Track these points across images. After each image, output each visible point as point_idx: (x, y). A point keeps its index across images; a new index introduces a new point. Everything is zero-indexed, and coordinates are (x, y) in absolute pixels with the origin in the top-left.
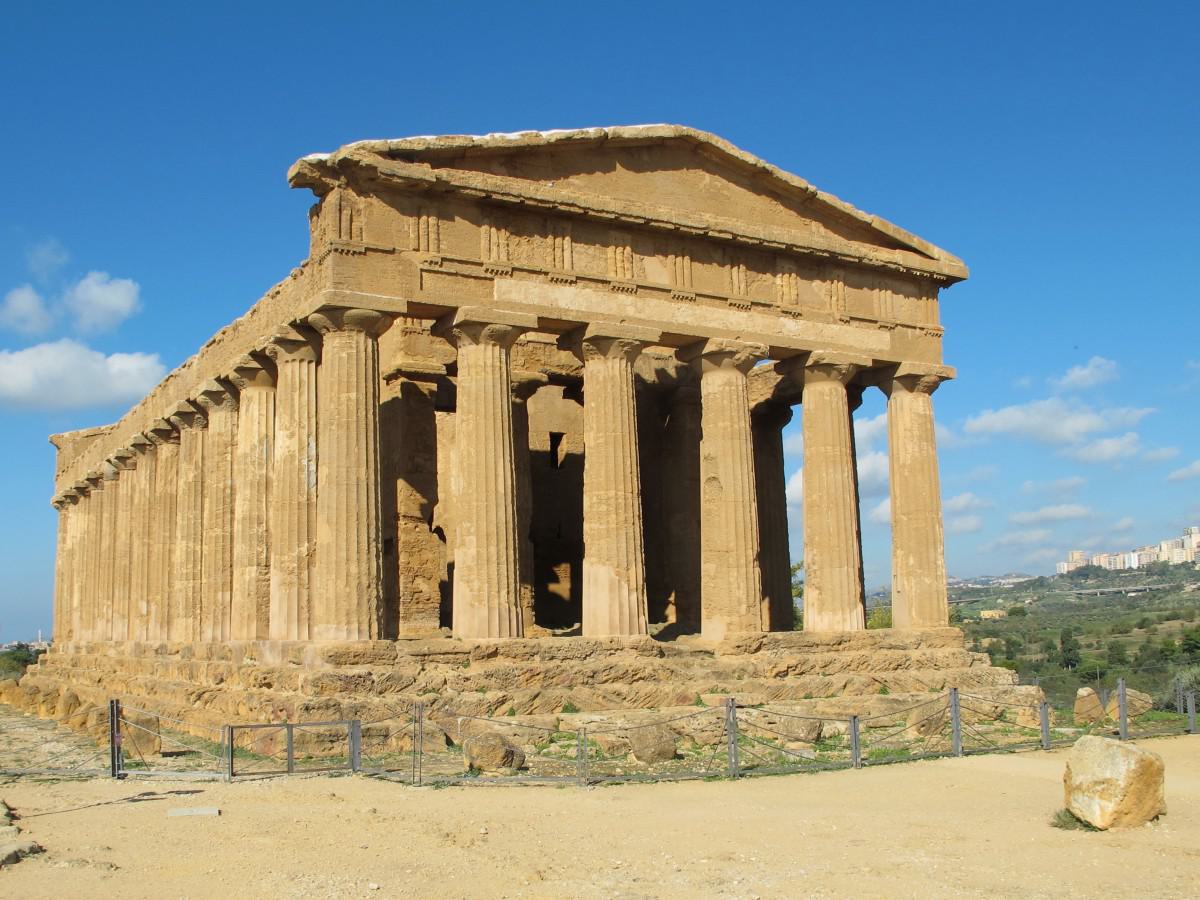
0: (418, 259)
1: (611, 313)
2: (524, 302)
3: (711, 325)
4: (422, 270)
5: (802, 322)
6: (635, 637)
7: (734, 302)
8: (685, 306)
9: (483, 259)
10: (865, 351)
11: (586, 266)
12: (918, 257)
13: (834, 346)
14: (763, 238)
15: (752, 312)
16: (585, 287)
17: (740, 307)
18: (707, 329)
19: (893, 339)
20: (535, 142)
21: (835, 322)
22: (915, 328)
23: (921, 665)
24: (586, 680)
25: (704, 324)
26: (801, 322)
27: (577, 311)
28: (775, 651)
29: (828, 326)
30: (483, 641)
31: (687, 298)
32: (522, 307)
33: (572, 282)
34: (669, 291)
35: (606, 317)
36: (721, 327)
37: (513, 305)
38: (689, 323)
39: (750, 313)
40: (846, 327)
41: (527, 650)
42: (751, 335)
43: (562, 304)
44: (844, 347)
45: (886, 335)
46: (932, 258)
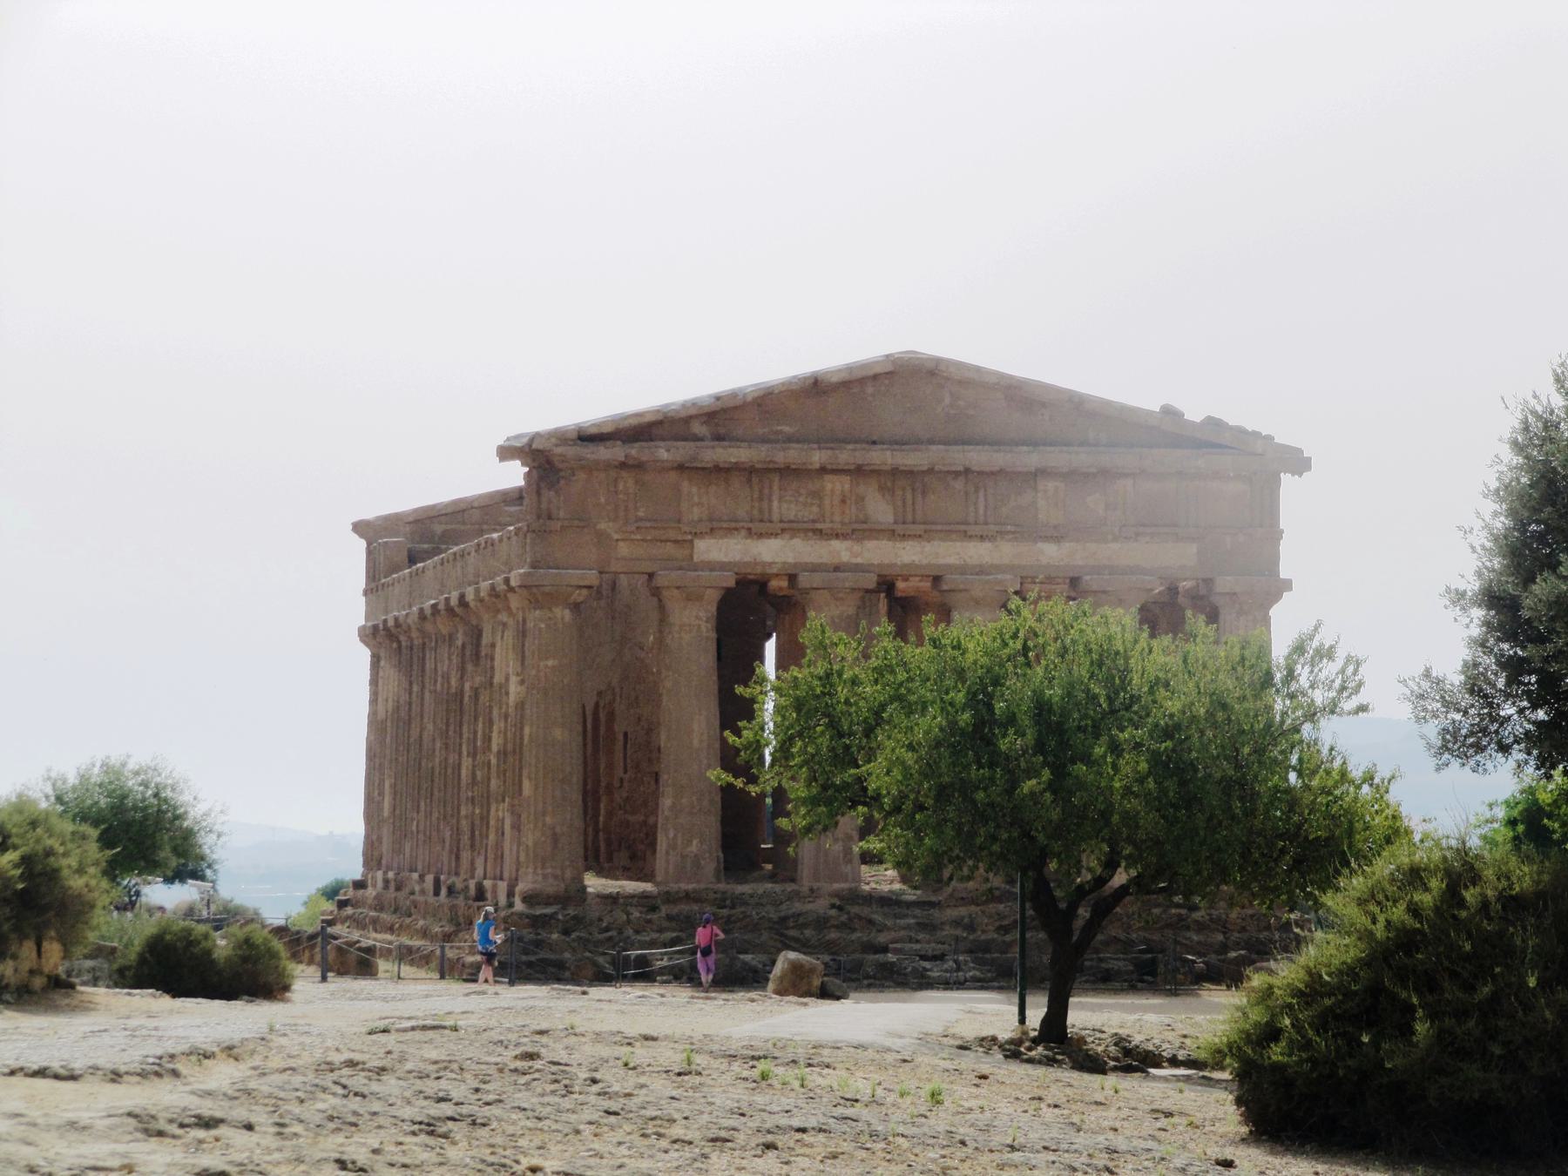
1: (820, 561)
2: (724, 560)
4: (617, 540)
5: (1067, 545)
6: (836, 886)
7: (974, 534)
11: (796, 516)
16: (792, 538)
17: (982, 538)
21: (1115, 539)
23: (1201, 927)
24: (771, 925)
26: (1067, 546)
27: (785, 563)
32: (723, 566)
33: (777, 535)
36: (958, 562)
38: (917, 562)
41: (715, 896)
43: (767, 558)
45: (1194, 548)
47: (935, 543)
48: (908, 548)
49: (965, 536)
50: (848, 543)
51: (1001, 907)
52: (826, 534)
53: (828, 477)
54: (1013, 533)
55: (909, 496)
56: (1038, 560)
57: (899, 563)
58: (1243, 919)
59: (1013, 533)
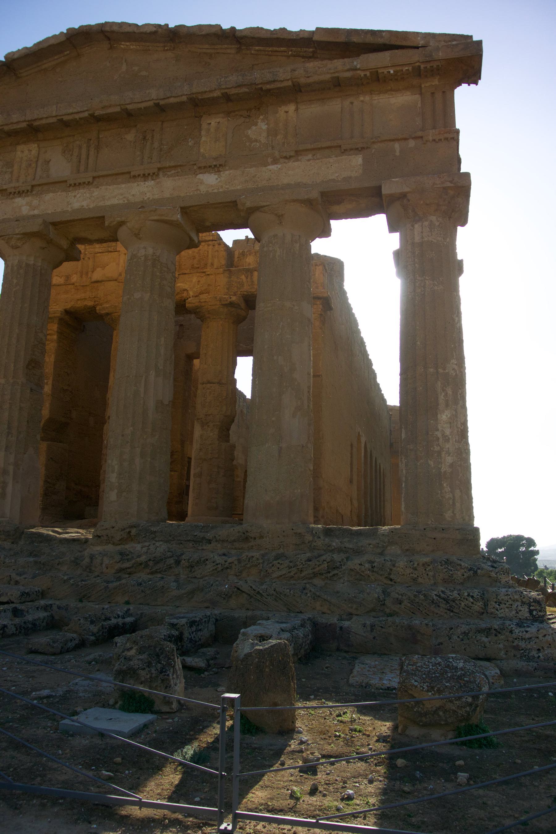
1: (5, 217)
3: (108, 203)
5: (227, 172)
7: (137, 173)
12: (387, 55)
14: (155, 98)
17: (145, 177)
22: (406, 139)
25: (101, 204)
26: (226, 174)
28: (147, 544)
29: (264, 169)
31: (84, 183)
34: (66, 181)
36: (121, 202)
39: (158, 180)
45: (358, 160)
46: (417, 48)
47: (103, 187)
48: (78, 196)
49: (130, 178)
50: (28, 199)
51: (138, 547)
52: (10, 193)
53: (20, 148)
54: (175, 167)
55: (84, 151)
56: (197, 190)
57: (70, 210)
58: (415, 569)
59: (175, 167)
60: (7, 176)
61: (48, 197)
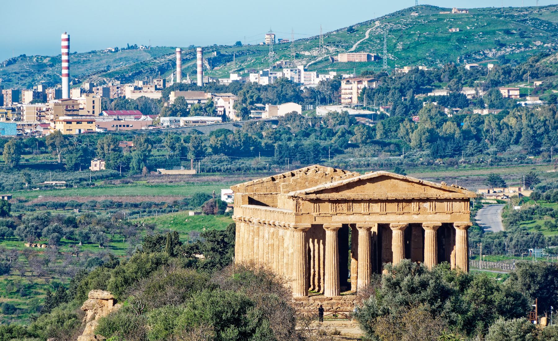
0: (315, 214)
8: (383, 216)
9: (330, 212)
10: (440, 221)
13: (431, 221)
15: (404, 215)
18: (390, 221)
19: (451, 216)
20: (341, 185)
26: (419, 216)
30: (329, 296)
35: (361, 222)
37: (336, 222)
40: (435, 215)
42: (403, 221)
43: (349, 220)
44: (434, 221)
45: (449, 216)
60: (360, 209)
61: (374, 216)
